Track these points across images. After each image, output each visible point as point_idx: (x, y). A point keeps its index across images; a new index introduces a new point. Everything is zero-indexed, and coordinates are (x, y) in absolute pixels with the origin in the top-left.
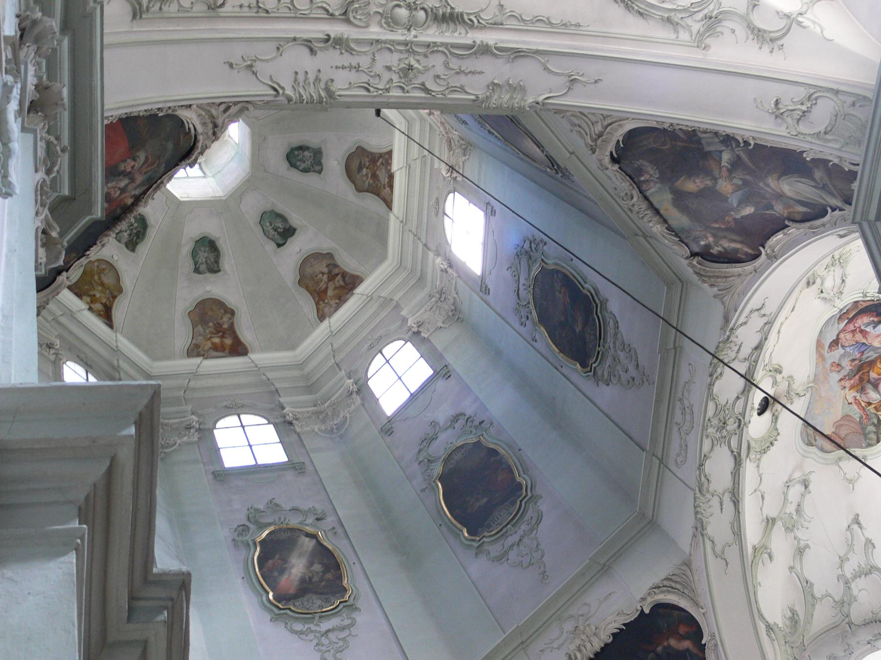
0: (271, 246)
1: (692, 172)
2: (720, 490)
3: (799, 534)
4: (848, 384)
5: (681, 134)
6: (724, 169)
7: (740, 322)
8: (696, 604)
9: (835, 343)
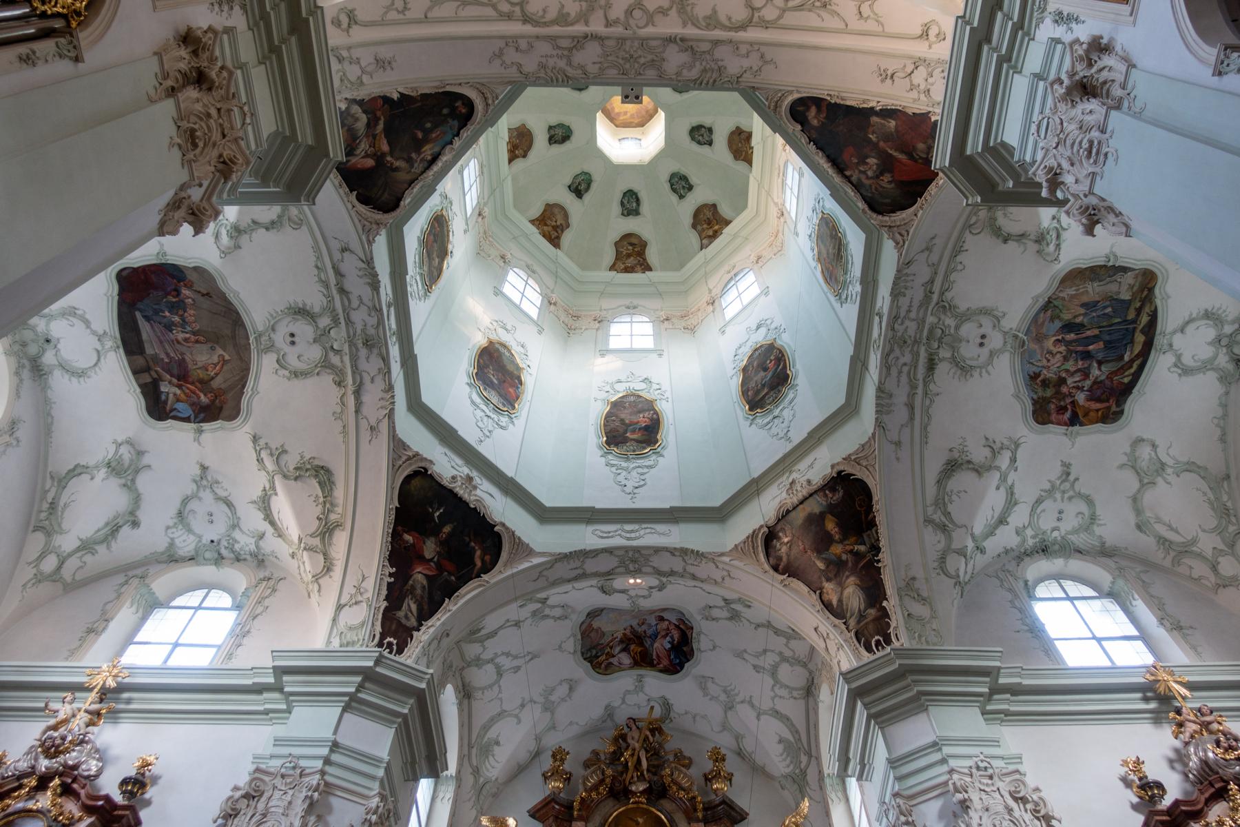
0: (568, 181)
1: (841, 525)
2: (585, 566)
3: (529, 621)
5: (871, 516)
6: (852, 547)
8: (505, 565)
9: (661, 619)
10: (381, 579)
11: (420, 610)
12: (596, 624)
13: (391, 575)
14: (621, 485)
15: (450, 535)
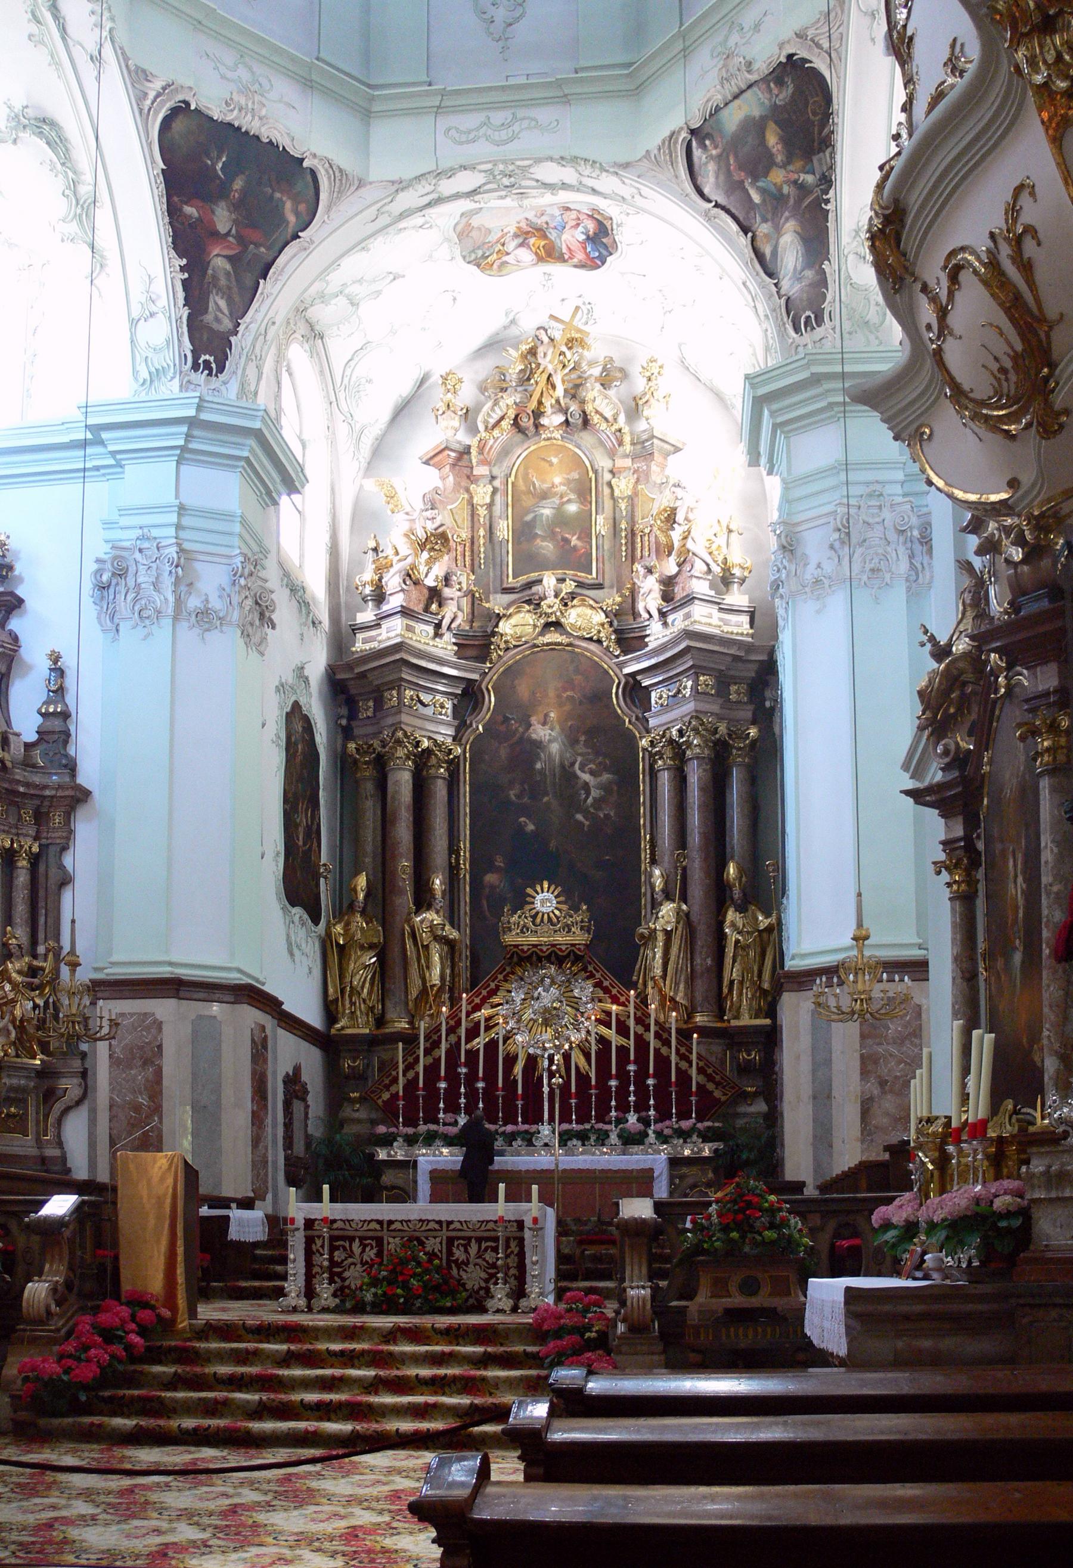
1: (787, 142)
4: (523, 225)
7: (626, 180)
9: (568, 209)
10: (172, 279)
11: (230, 301)
12: (475, 222)
13: (182, 269)
14: (484, 20)
15: (244, 192)
